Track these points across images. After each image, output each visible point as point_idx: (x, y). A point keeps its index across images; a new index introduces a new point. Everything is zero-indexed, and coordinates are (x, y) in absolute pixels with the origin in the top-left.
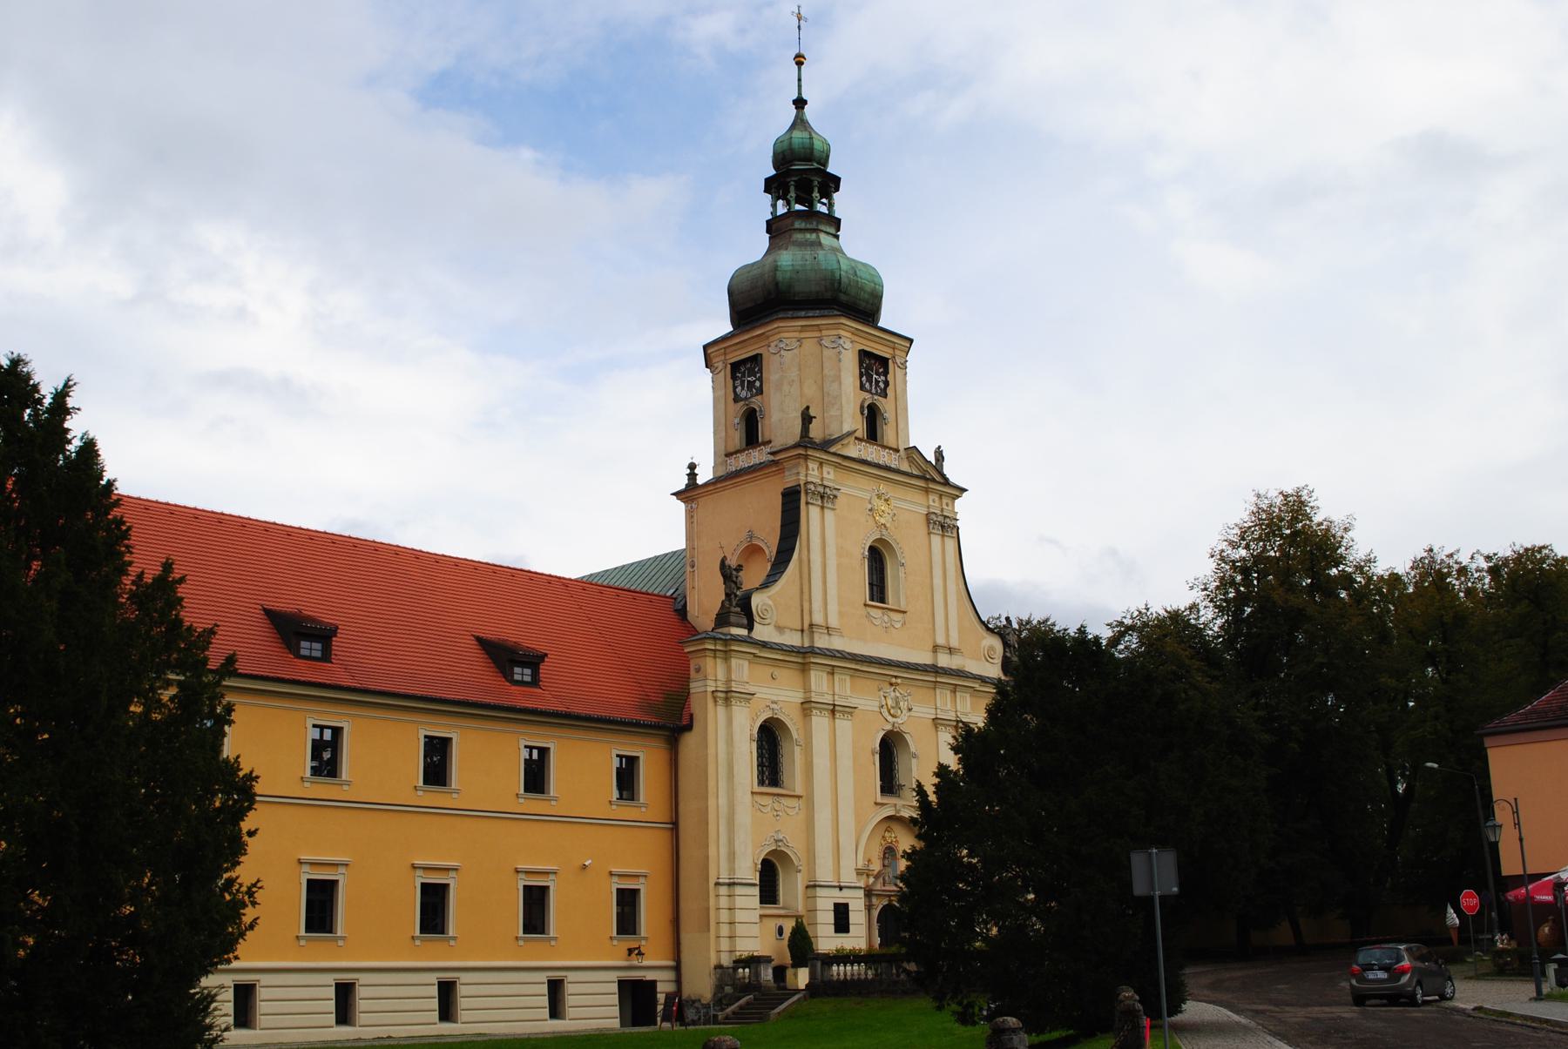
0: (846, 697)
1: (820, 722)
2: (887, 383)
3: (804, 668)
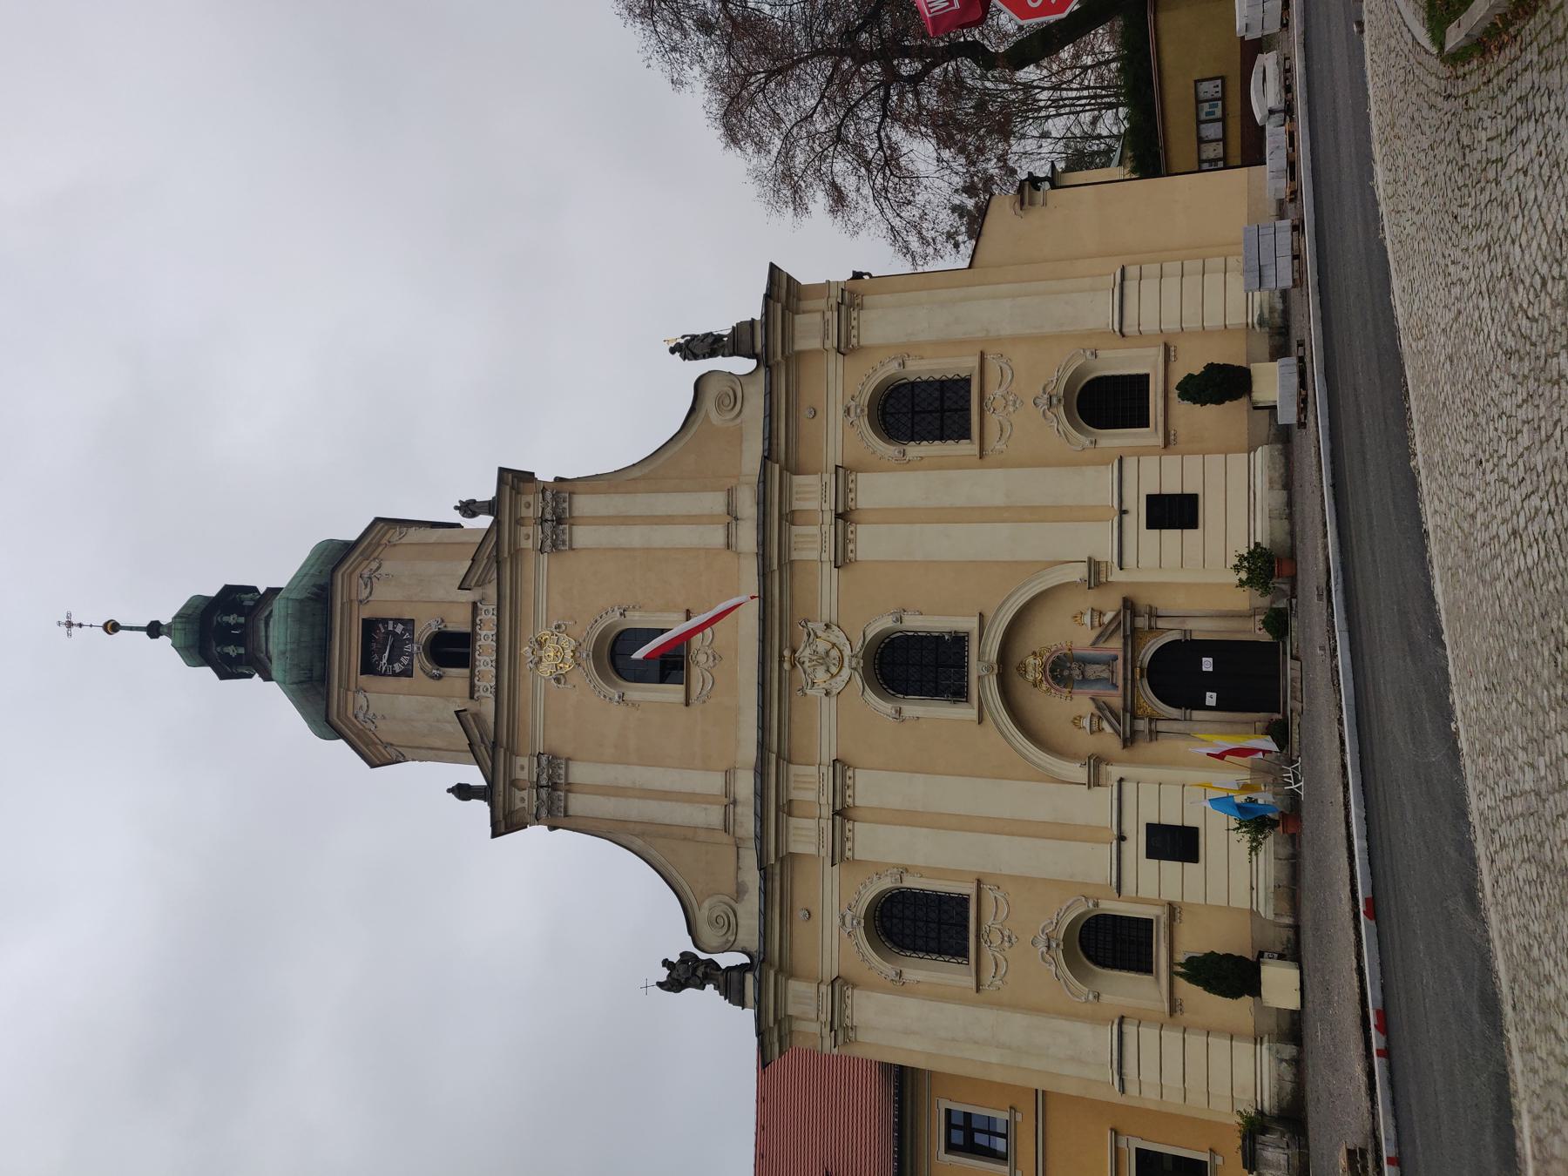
0: (821, 776)
1: (869, 841)
2: (397, 621)
3: (788, 860)
